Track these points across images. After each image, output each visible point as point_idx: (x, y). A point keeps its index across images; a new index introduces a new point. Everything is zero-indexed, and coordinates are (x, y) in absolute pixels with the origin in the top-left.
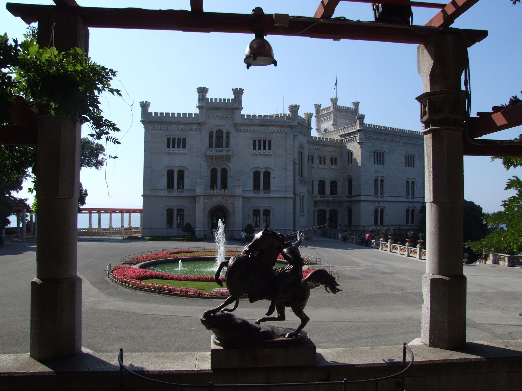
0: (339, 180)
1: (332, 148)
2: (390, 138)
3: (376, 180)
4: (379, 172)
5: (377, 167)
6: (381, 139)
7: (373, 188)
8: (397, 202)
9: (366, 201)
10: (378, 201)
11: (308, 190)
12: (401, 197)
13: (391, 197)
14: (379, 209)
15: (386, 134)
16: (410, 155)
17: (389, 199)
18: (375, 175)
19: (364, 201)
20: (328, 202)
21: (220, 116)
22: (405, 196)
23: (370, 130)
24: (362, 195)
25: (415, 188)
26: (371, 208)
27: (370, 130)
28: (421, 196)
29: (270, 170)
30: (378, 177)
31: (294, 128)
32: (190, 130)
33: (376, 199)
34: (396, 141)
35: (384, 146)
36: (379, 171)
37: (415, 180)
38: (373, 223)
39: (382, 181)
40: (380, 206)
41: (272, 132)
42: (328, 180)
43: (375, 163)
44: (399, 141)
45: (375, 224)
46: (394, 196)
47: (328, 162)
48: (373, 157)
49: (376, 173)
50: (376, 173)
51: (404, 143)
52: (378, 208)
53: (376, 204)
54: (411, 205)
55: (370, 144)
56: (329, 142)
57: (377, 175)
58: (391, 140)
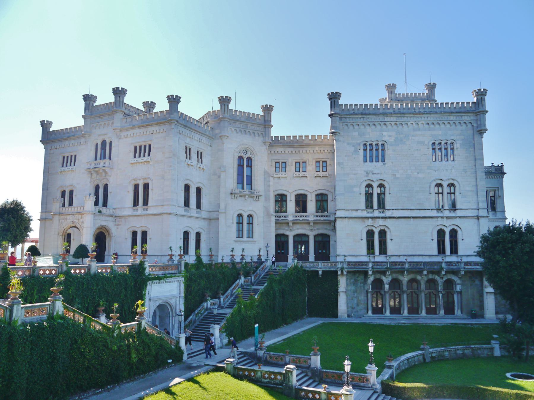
0: (331, 192)
1: (317, 149)
2: (395, 120)
4: (373, 174)
5: (370, 166)
7: (363, 199)
8: (413, 217)
11: (264, 207)
12: (424, 211)
17: (396, 214)
18: (366, 178)
20: (308, 223)
21: (103, 124)
23: (354, 112)
26: (361, 229)
27: (354, 112)
28: (475, 207)
29: (148, 181)
30: (373, 181)
31: (171, 123)
34: (409, 123)
35: (385, 133)
36: (374, 172)
37: (457, 181)
38: (364, 251)
40: (376, 226)
41: (152, 134)
42: (310, 192)
43: (365, 161)
44: (417, 122)
46: (408, 210)
48: (361, 152)
50: (367, 176)
51: (428, 124)
53: (370, 222)
55: (356, 134)
56: (311, 140)
57: (369, 178)
58: (397, 123)
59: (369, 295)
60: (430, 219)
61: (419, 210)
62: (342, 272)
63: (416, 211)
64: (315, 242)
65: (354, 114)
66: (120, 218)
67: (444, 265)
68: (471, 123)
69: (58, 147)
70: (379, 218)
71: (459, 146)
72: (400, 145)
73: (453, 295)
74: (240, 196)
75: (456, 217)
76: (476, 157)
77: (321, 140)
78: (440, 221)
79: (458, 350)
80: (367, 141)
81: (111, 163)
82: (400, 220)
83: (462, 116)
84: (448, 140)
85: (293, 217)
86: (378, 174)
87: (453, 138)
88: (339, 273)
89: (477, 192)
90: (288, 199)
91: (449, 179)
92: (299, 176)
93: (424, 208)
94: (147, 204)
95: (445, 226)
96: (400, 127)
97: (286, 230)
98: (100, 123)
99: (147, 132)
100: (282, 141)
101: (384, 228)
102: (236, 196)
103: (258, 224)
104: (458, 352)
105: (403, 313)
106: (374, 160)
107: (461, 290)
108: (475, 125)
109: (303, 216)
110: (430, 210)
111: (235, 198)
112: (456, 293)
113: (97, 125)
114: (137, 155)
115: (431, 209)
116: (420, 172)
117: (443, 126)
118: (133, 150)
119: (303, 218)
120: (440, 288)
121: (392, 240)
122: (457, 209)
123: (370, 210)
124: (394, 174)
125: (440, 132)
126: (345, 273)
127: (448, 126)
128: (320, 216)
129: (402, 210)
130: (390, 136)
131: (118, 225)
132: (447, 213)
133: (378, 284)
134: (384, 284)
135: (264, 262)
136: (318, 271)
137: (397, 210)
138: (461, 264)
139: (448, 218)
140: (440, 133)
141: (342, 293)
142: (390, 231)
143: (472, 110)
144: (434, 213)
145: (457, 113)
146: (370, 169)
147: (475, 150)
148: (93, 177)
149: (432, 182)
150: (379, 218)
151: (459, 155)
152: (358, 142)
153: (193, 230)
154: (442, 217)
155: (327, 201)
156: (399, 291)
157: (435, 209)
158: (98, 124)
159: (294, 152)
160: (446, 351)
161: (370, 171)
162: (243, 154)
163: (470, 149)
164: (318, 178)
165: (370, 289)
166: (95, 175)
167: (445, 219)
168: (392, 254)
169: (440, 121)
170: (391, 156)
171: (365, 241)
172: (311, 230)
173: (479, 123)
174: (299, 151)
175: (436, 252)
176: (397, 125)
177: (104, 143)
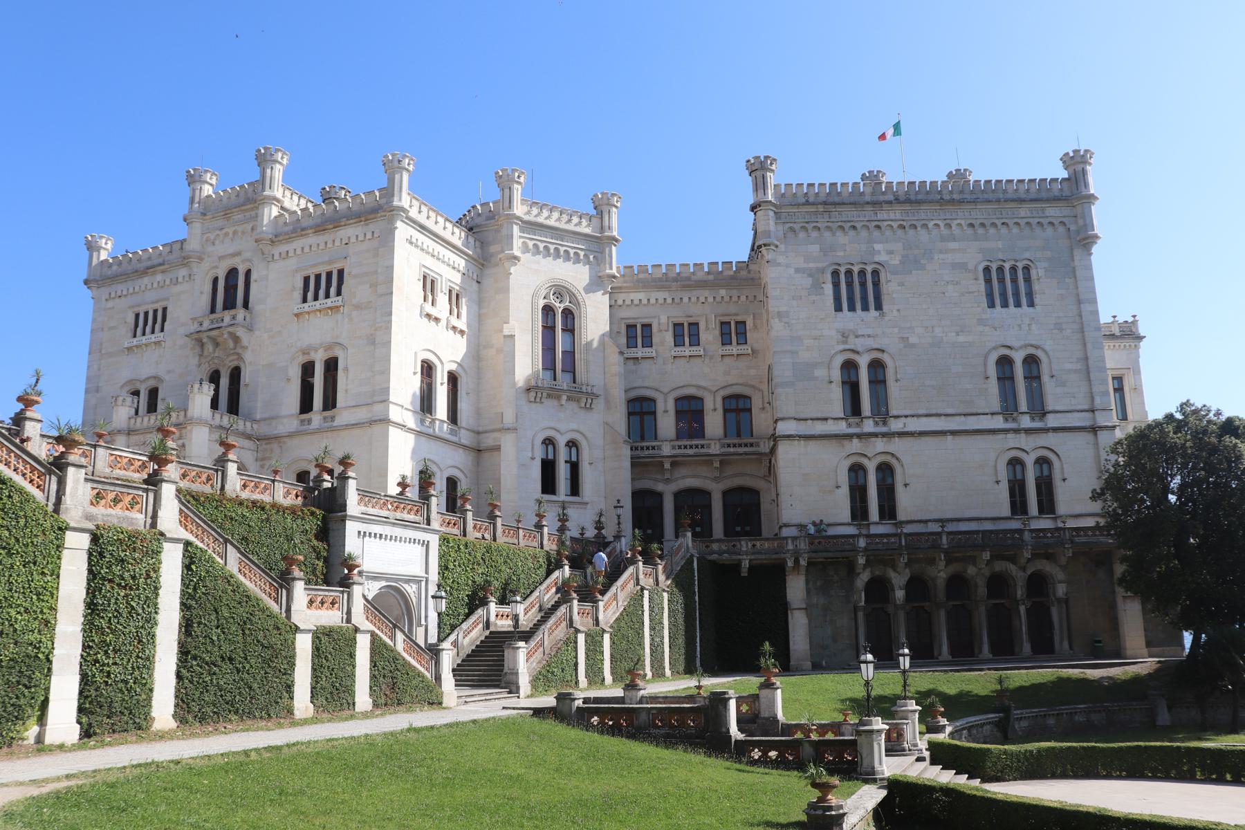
1: (723, 292)
2: (898, 216)
3: (849, 366)
4: (857, 337)
5: (848, 319)
6: (858, 225)
8: (954, 433)
9: (800, 436)
10: (859, 436)
13: (924, 420)
14: (871, 467)
15: (876, 204)
16: (1007, 266)
17: (914, 425)
18: (842, 347)
19: (788, 437)
20: (707, 460)
21: (230, 231)
22: (997, 408)
23: (807, 201)
24: (782, 419)
25: (1045, 378)
27: (807, 201)
28: (1086, 407)
30: (858, 353)
32: (175, 284)
33: (851, 431)
34: (931, 224)
35: (878, 247)
36: (860, 332)
38: (845, 514)
39: (877, 366)
40: (869, 455)
41: (347, 244)
42: (710, 391)
43: (838, 308)
44: (947, 221)
45: (854, 516)
46: (939, 415)
47: (710, 335)
48: (829, 289)
49: (845, 342)
50: (845, 342)
51: (972, 225)
52: (865, 461)
53: (855, 446)
54: (1030, 448)
55: (814, 249)
56: (708, 273)
57: (847, 347)
58: (904, 223)
59: (861, 615)
60: (991, 437)
61: (964, 415)
62: (797, 561)
63: (958, 418)
64: (725, 506)
65: (807, 203)
66: (266, 444)
67: (1027, 536)
68: (1063, 223)
69: (125, 293)
70: (875, 435)
71: (1041, 272)
72: (914, 272)
73: (1048, 609)
74: (549, 396)
75: (1046, 430)
76: (1082, 297)
77: (731, 273)
78: (1012, 440)
79: (1076, 713)
80: (839, 265)
81: (247, 319)
82: (925, 439)
83: (1043, 209)
84: (1017, 261)
85: (674, 448)
86: (869, 336)
87: (1027, 255)
88: (790, 563)
89: (1089, 373)
90: (660, 407)
91: (1026, 346)
92: (683, 354)
93: (974, 411)
94: (334, 406)
95: (1023, 450)
96: (911, 232)
97: (657, 480)
98: (224, 231)
99: (334, 241)
100: (641, 276)
101: (888, 458)
102: (539, 395)
103: (591, 464)
104: (1077, 718)
105: (940, 654)
106: (858, 305)
107: (1066, 595)
108: (1073, 228)
109: (697, 447)
110: (989, 416)
111: (538, 400)
112: (1056, 603)
113: (218, 235)
114: (310, 295)
115: (992, 414)
116: (962, 331)
117: (1004, 230)
118: (300, 284)
119: (697, 450)
120: (1019, 593)
121: (908, 487)
122: (1048, 413)
123: (853, 420)
124: (905, 336)
125: (1000, 243)
126: (803, 563)
127: (1015, 230)
128: (735, 446)
129: (927, 415)
130: (890, 252)
131: (263, 459)
132: (1026, 422)
133: (878, 589)
134: (893, 590)
135: (610, 542)
136: (740, 561)
137: (915, 418)
138: (1064, 532)
139: (1028, 431)
140: (1000, 244)
141: (797, 611)
142: (902, 465)
143: (1064, 195)
144: (998, 422)
145: (1032, 200)
146: (851, 326)
147: (1076, 281)
148: (206, 353)
149: (990, 351)
150: (875, 435)
151: (1044, 293)
152: (820, 265)
153: (441, 470)
154: (1017, 431)
155: (750, 410)
156: (927, 604)
157: (1000, 414)
158: (218, 232)
159: (669, 301)
160: (1049, 715)
161: (851, 330)
162: (553, 302)
163: (1067, 280)
164: (727, 360)
165: (861, 602)
166: (209, 347)
167: (1023, 435)
168: (909, 519)
169: (998, 218)
170: (894, 295)
171: (844, 491)
172: (716, 479)
173: (1081, 222)
174: (681, 299)
175: (1006, 511)
176: (904, 228)
177: (232, 273)
